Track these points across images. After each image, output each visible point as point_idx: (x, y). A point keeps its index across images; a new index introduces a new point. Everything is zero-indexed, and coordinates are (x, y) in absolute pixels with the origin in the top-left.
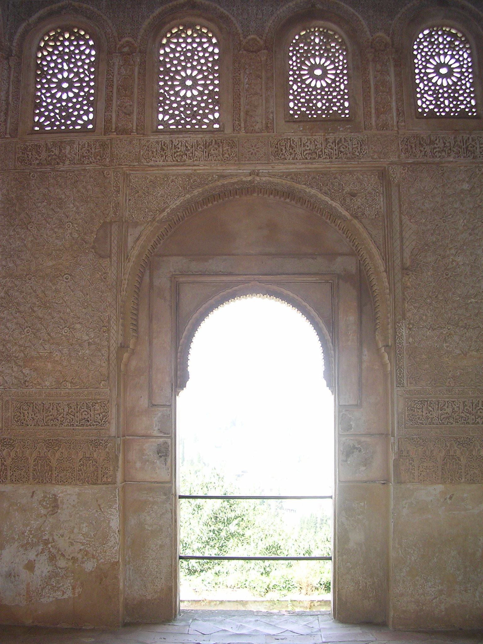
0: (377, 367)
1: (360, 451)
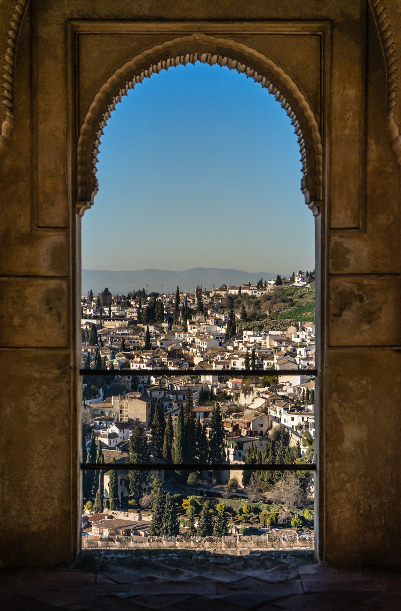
0: (390, 170)
1: (361, 300)
